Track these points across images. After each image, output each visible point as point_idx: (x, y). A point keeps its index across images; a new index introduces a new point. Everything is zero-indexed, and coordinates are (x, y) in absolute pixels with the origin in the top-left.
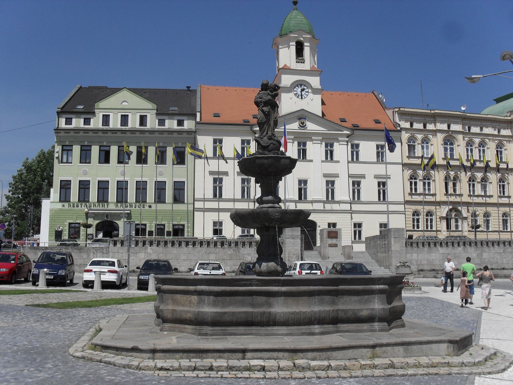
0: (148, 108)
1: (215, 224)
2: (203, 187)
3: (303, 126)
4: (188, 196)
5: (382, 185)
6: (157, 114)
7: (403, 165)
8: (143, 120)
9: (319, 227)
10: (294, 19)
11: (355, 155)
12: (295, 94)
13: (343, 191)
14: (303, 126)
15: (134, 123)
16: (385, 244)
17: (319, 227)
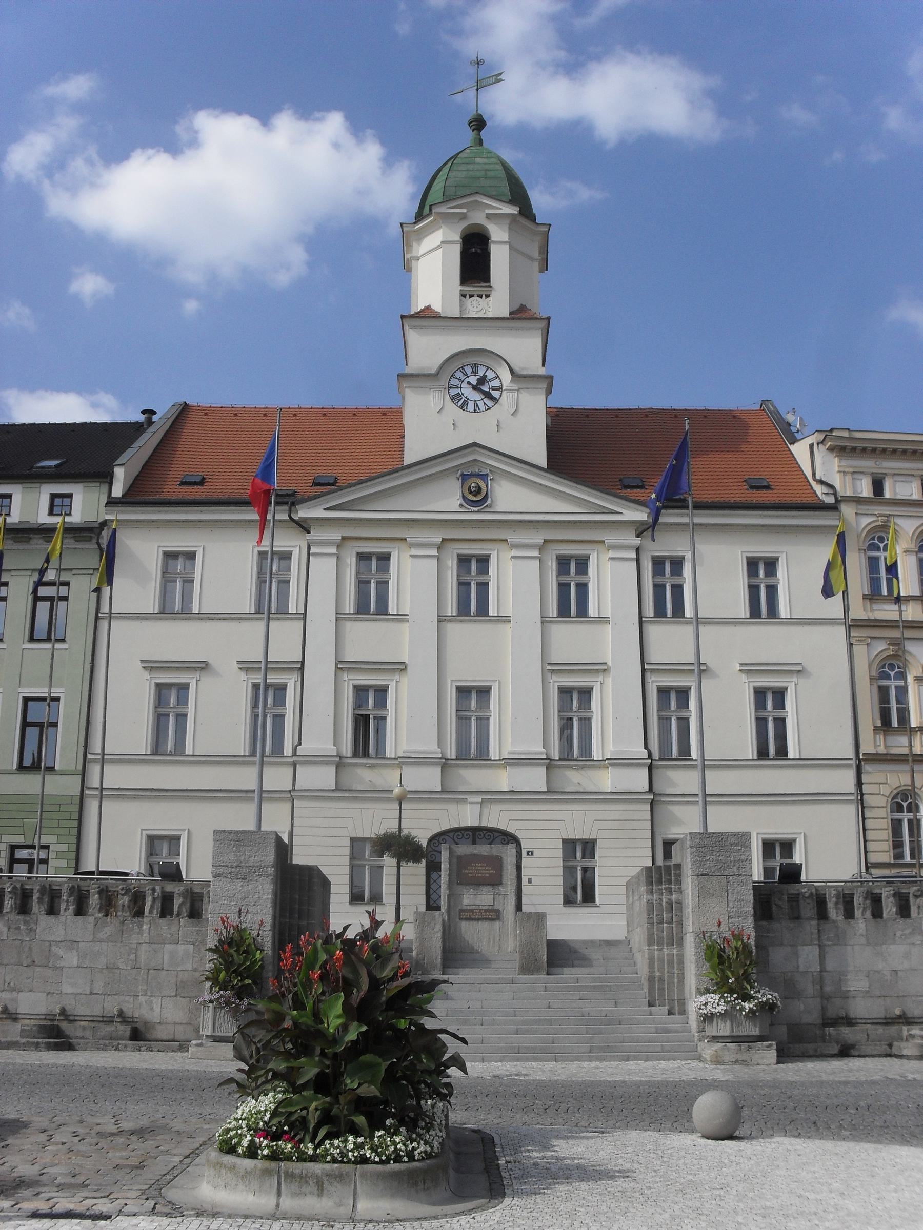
3: (477, 497)
4: (64, 749)
5: (769, 700)
7: (850, 628)
9: (530, 854)
10: (463, 167)
11: (665, 598)
12: (453, 399)
13: (617, 725)
14: (477, 497)
16: (670, 903)
17: (530, 854)
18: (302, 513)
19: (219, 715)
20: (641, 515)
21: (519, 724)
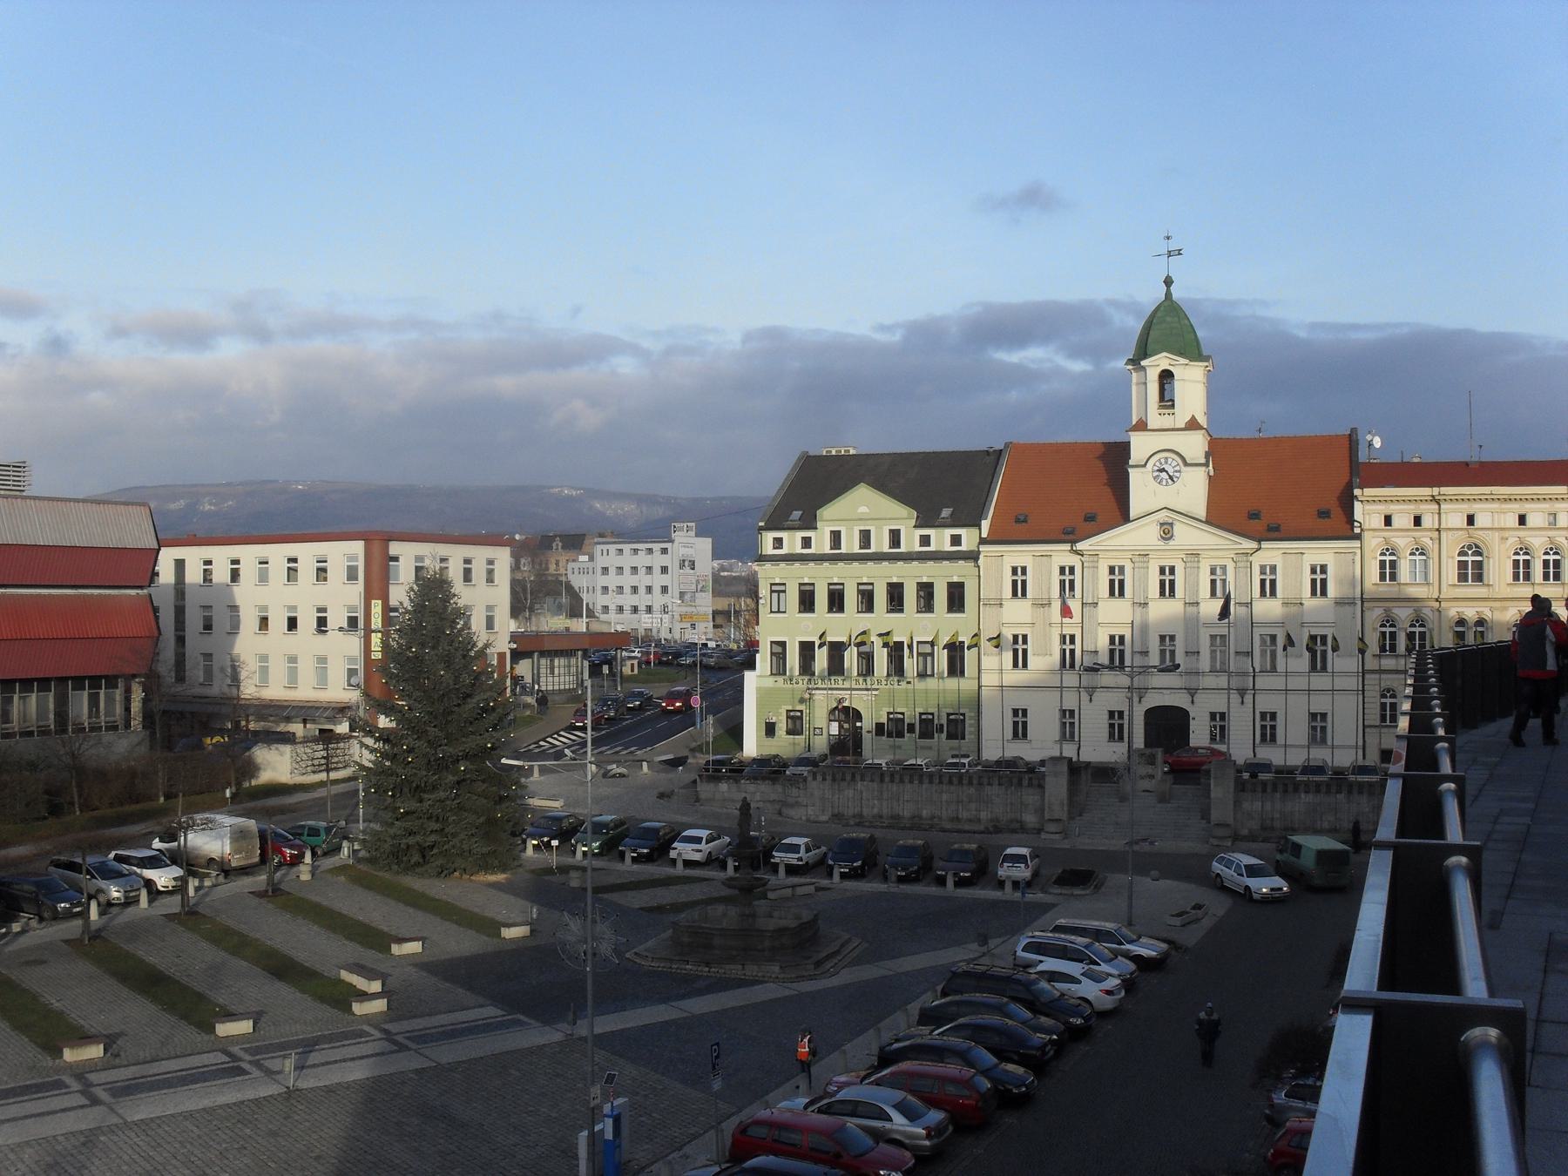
0: (901, 516)
3: (1167, 532)
8: (895, 537)
15: (881, 543)
18: (1080, 546)
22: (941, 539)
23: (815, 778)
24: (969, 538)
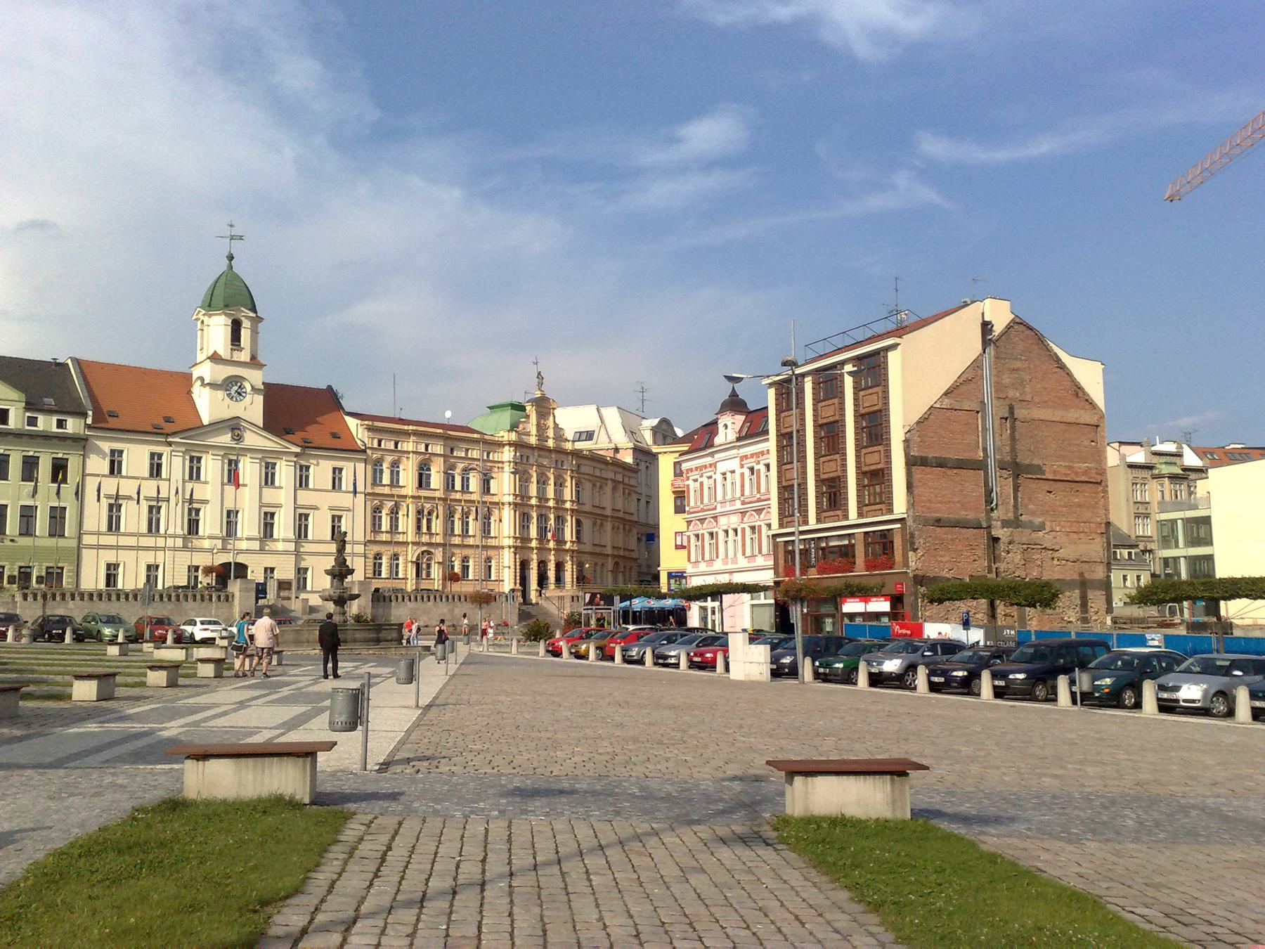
1: (109, 566)
2: (96, 516)
6: (27, 409)
11: (302, 481)
13: (284, 526)
19: (134, 517)
20: (298, 450)
21: (248, 525)
22: (47, 423)
23: (25, 597)
24: (73, 426)
